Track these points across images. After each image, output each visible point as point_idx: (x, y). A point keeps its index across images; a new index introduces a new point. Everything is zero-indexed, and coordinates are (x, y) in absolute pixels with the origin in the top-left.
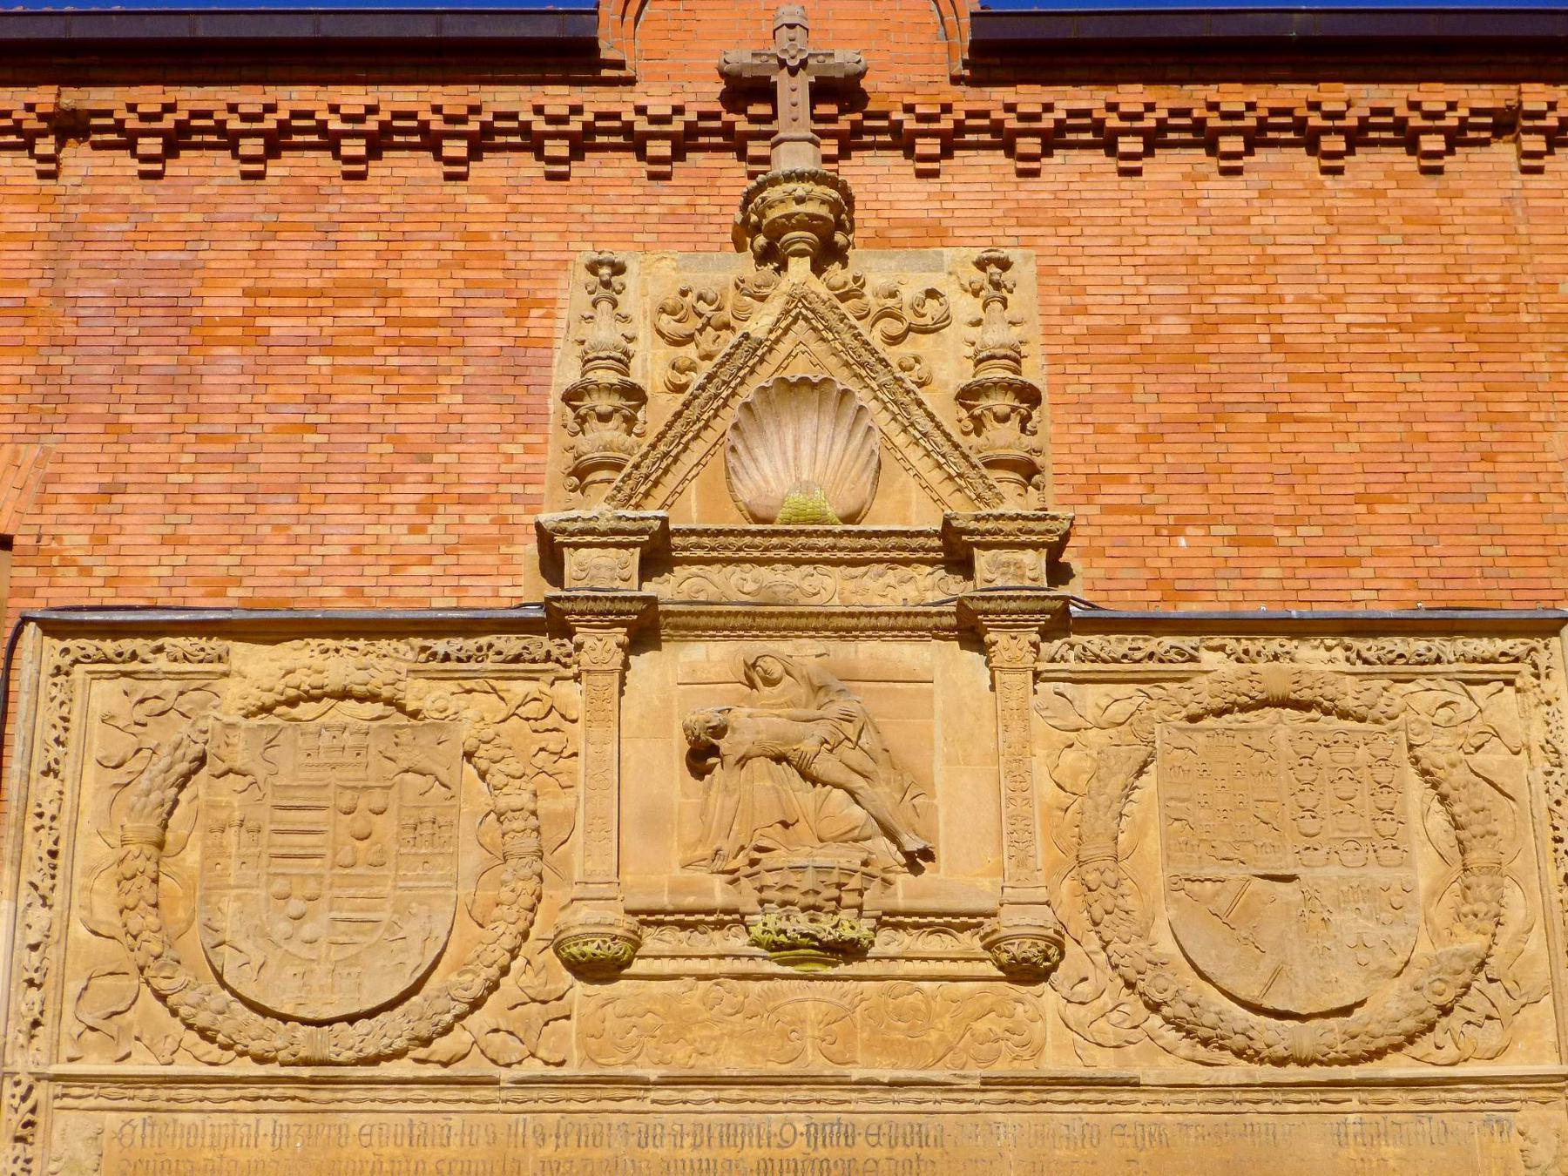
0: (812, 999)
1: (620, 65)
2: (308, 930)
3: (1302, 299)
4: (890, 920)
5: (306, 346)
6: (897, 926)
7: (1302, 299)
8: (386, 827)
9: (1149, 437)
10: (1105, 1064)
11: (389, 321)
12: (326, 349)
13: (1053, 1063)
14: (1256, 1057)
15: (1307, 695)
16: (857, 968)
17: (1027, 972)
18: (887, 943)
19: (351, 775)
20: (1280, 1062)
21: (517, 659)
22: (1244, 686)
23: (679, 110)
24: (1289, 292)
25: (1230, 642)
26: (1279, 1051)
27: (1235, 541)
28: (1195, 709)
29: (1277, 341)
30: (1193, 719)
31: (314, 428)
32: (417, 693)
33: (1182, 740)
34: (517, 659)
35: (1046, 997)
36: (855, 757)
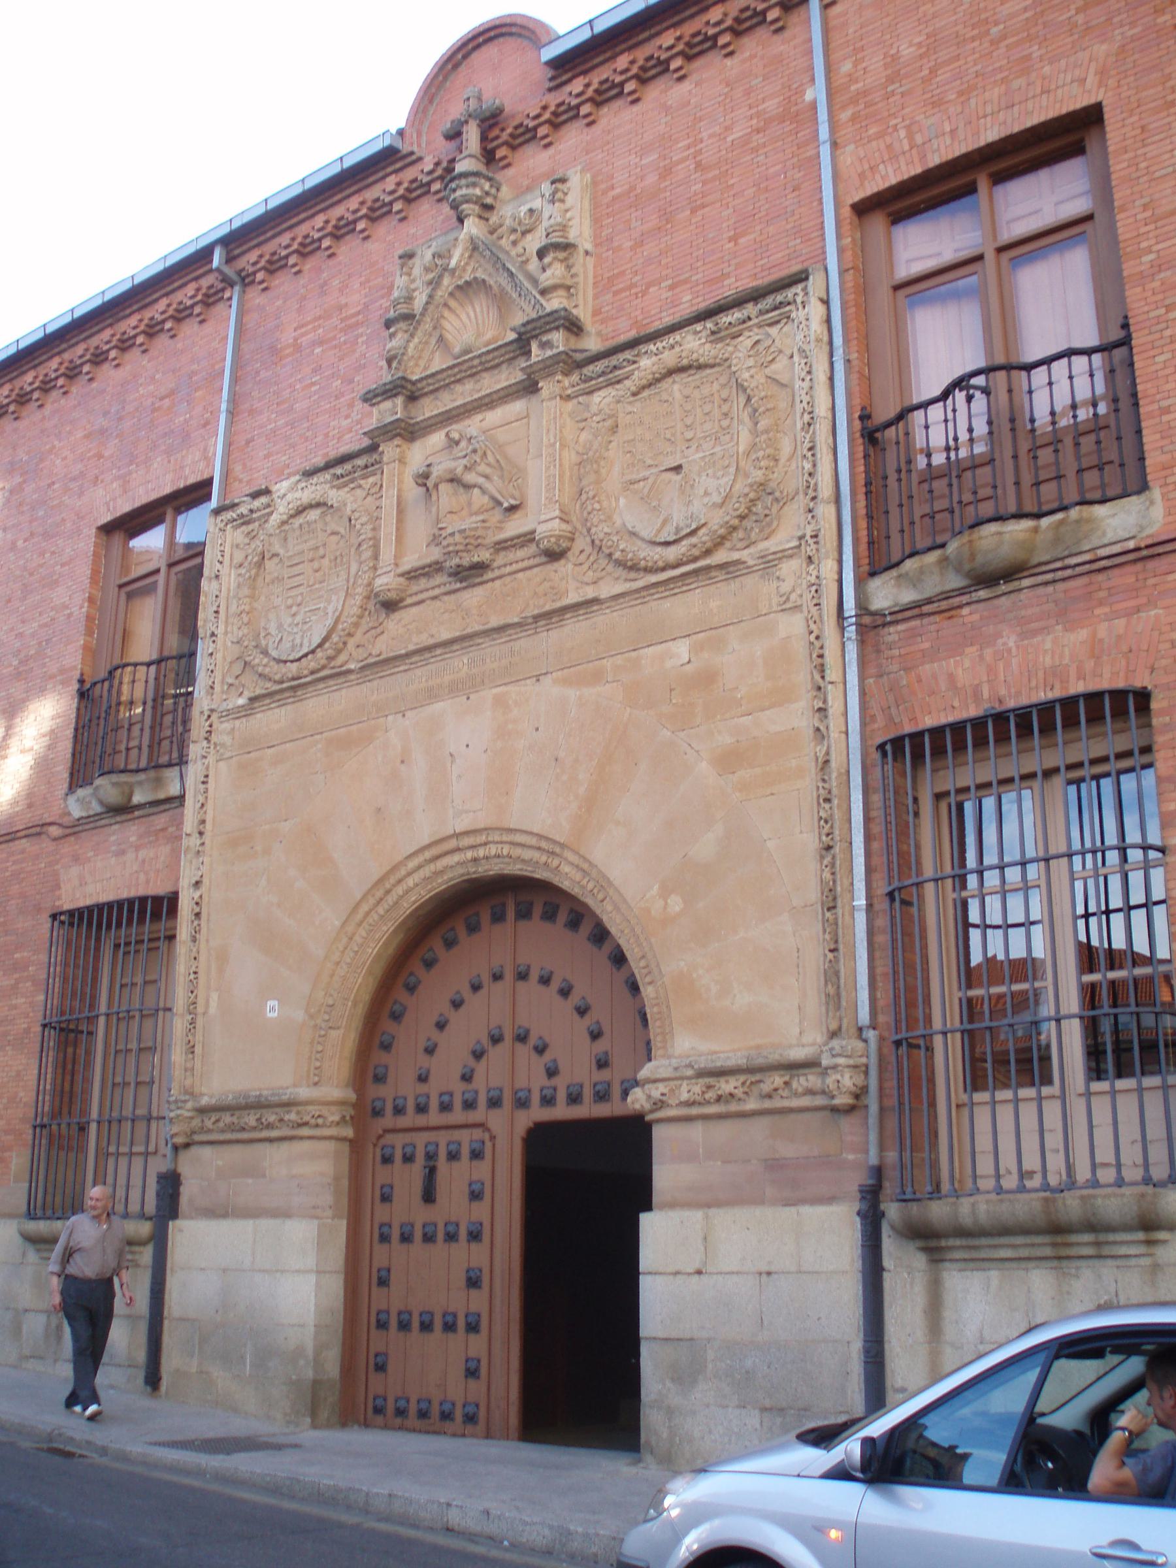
0: (473, 597)
1: (412, 153)
2: (298, 618)
3: (710, 136)
4: (502, 546)
5: (314, 344)
6: (505, 549)
7: (710, 136)
8: (326, 562)
9: (639, 243)
10: (590, 593)
11: (342, 320)
12: (321, 343)
13: (572, 598)
14: (648, 570)
15: (685, 362)
16: (490, 575)
17: (554, 555)
18: (501, 559)
19: (311, 543)
20: (663, 569)
21: (366, 467)
22: (655, 369)
23: (437, 164)
24: (704, 135)
25: (652, 347)
26: (661, 564)
27: (672, 288)
28: (633, 389)
29: (698, 165)
30: (634, 394)
31: (314, 384)
32: (334, 496)
33: (629, 408)
34: (366, 467)
35: (564, 568)
36: (482, 468)
